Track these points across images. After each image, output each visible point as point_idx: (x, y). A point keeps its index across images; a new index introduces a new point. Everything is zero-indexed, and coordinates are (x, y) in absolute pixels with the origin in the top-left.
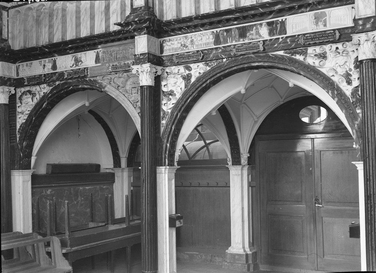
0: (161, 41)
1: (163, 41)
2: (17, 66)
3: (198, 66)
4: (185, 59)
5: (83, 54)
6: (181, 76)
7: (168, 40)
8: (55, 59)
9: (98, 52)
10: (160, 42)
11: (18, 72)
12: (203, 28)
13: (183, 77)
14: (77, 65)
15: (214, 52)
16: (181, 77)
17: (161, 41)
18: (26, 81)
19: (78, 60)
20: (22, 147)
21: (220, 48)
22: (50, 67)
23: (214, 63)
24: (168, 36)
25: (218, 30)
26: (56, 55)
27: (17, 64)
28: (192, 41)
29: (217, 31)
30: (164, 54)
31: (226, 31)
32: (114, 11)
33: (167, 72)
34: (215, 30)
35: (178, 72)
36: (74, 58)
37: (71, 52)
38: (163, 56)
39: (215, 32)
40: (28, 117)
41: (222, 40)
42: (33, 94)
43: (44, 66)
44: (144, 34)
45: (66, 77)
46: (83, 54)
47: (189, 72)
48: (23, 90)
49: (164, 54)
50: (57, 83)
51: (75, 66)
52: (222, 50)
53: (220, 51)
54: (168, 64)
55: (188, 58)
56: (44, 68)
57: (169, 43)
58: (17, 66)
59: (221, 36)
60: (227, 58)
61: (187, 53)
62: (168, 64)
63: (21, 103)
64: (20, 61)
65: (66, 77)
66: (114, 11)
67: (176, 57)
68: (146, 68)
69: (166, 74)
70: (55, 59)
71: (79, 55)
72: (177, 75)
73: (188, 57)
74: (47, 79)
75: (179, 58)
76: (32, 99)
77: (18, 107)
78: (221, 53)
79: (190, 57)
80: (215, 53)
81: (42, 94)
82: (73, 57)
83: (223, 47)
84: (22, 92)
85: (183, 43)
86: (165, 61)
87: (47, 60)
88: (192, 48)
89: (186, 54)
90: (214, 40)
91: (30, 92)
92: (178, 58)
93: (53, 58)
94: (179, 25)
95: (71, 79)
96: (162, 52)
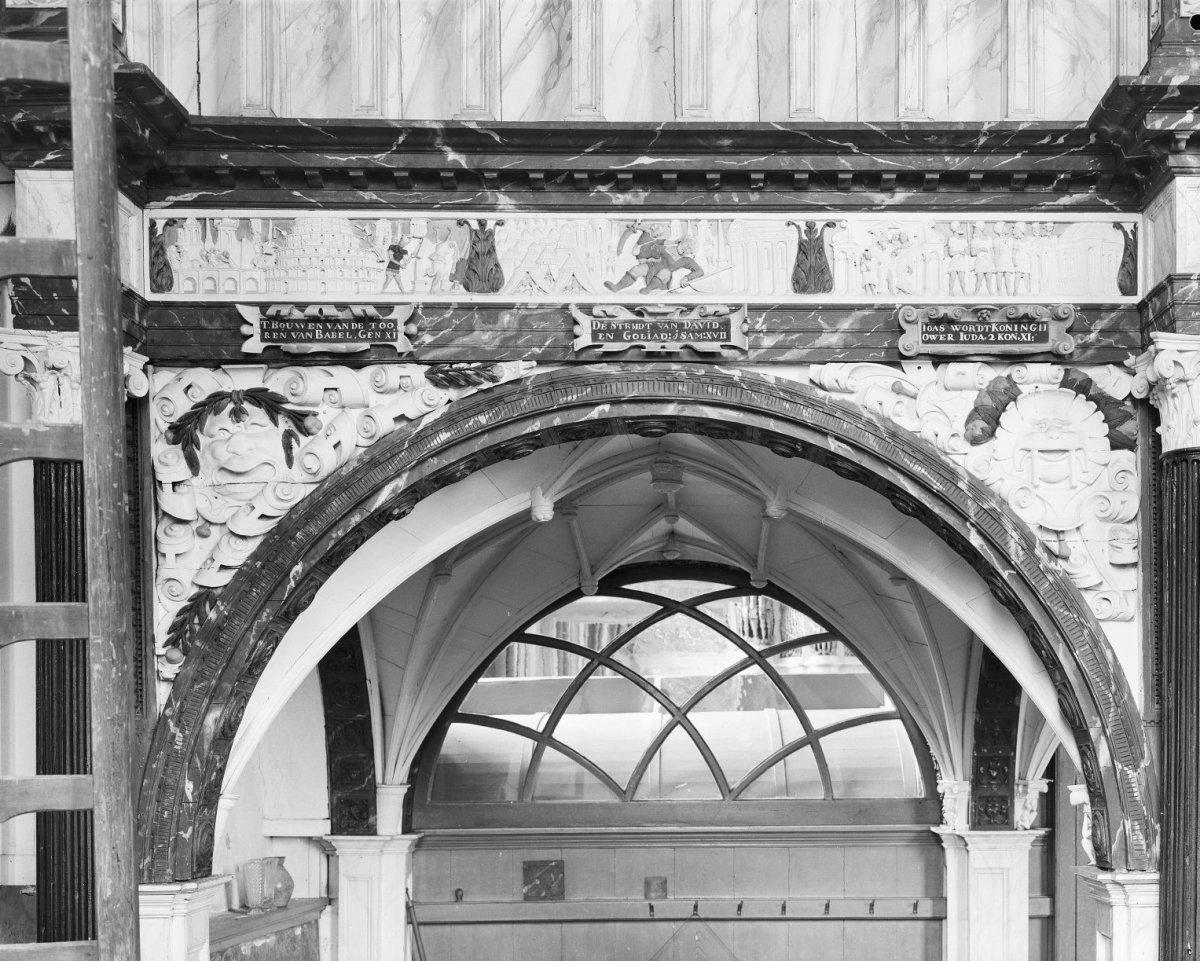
2: (153, 224)
5: (703, 226)
8: (482, 223)
9: (810, 227)
11: (167, 265)
14: (652, 282)
18: (256, 330)
19: (663, 256)
20: (199, 737)
22: (447, 267)
26: (503, 199)
27: (160, 213)
32: (958, 15)
36: (635, 237)
37: (621, 198)
40: (255, 556)
42: (298, 418)
43: (398, 252)
45: (585, 340)
46: (703, 226)
48: (206, 381)
50: (507, 371)
51: (640, 283)
56: (393, 267)
58: (153, 224)
63: (193, 464)
64: (189, 196)
65: (585, 340)
66: (958, 15)
70: (482, 223)
71: (672, 226)
74: (428, 339)
76: (288, 448)
77: (168, 488)
81: (385, 424)
82: (631, 229)
84: (201, 397)
87: (419, 219)
91: (271, 404)
93: (472, 217)
95: (610, 357)
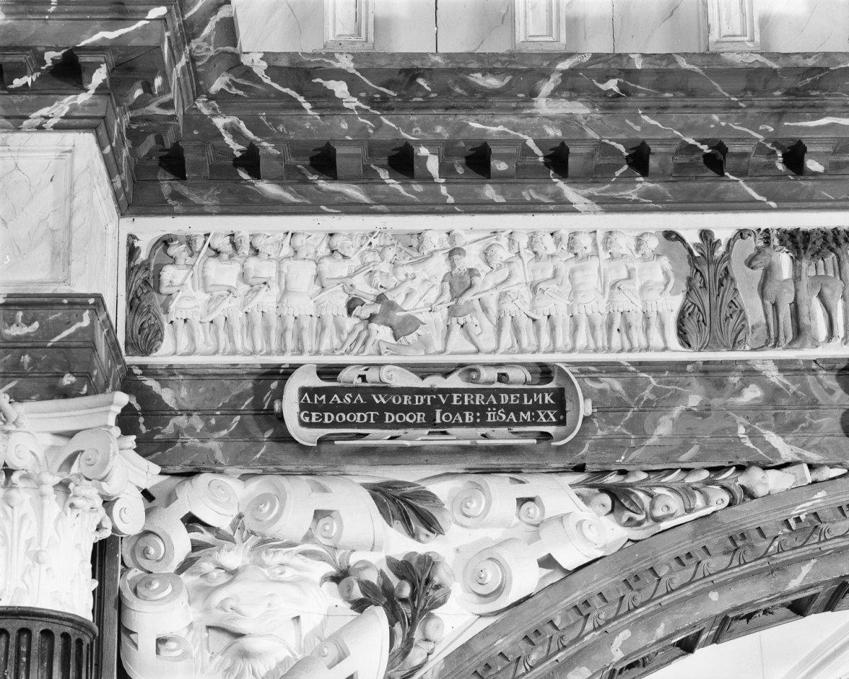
0: (144, 245)
1: (166, 242)
3: (522, 501)
4: (395, 426)
6: (330, 569)
7: (222, 243)
10: (132, 251)
12: (593, 190)
13: (366, 586)
15: (694, 401)
16: (336, 579)
17: (144, 245)
21: (750, 373)
23: (687, 492)
24: (227, 209)
25: (724, 225)
28: (460, 284)
29: (705, 234)
30: (162, 356)
31: (798, 242)
33: (191, 521)
34: (689, 225)
35: (308, 538)
38: (168, 374)
39: (692, 238)
41: (754, 310)
44: (57, 128)
47: (420, 548)
49: (162, 356)
52: (774, 394)
53: (752, 394)
54: (212, 444)
55: (430, 422)
57: (224, 273)
59: (745, 281)
60: (811, 467)
61: (423, 370)
62: (212, 444)
67: (303, 390)
68: (61, 442)
69: (181, 541)
72: (299, 561)
73: (429, 411)
75: (335, 409)
78: (753, 411)
79: (455, 410)
80: (704, 412)
83: (782, 366)
85: (363, 288)
86: (181, 421)
88: (457, 339)
89: (413, 381)
90: (677, 302)
92: (321, 408)
94: (380, 125)
96: (146, 338)
